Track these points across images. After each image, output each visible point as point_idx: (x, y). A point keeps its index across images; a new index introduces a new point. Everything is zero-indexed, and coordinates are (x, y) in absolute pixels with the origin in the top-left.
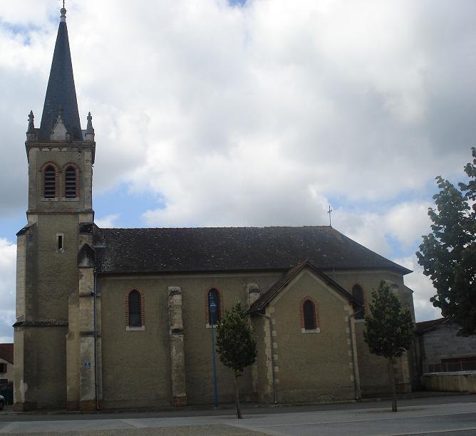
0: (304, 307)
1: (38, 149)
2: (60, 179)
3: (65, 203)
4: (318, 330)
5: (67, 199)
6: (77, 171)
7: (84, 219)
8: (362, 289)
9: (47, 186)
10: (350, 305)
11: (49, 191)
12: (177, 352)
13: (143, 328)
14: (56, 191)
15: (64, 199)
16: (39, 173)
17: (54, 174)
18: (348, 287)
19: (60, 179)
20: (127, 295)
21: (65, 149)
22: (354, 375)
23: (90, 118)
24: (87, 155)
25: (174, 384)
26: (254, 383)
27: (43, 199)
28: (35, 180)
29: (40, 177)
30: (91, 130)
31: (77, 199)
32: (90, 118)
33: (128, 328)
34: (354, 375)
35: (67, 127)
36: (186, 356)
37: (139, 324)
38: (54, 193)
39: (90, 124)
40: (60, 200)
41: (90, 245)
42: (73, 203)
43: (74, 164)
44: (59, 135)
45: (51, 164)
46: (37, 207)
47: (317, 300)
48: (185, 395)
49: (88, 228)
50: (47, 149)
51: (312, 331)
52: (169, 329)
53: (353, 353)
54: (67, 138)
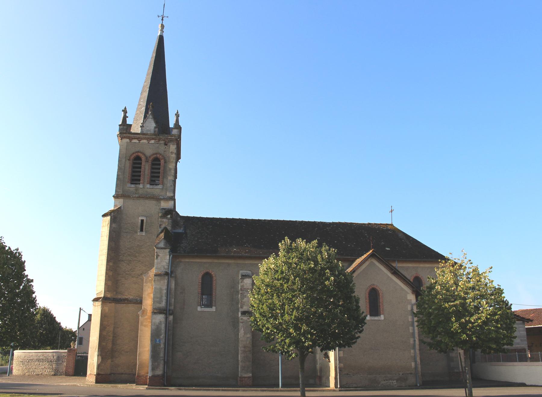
0: (369, 294)
1: (128, 140)
2: (146, 168)
3: (149, 190)
4: (382, 317)
5: (151, 187)
6: (162, 162)
7: (165, 205)
8: (421, 280)
9: (134, 174)
10: (413, 293)
11: (135, 178)
12: (245, 333)
13: (214, 309)
14: (142, 178)
15: (148, 186)
16: (128, 161)
17: (141, 164)
18: (411, 277)
19: (146, 168)
20: (200, 276)
21: (153, 141)
22: (416, 362)
23: (177, 115)
24: (173, 148)
25: (240, 364)
26: (318, 366)
27: (129, 185)
28: (123, 168)
29: (128, 164)
30: (178, 126)
31: (160, 187)
32: (177, 115)
33: (199, 309)
34: (416, 362)
35: (156, 122)
36: (253, 337)
37: (210, 305)
38: (139, 180)
39: (177, 121)
40: (145, 187)
41: (169, 228)
42: (157, 190)
43: (160, 154)
44: (148, 128)
45: (139, 154)
46: (123, 191)
47: (382, 288)
48: (251, 375)
49: (171, 212)
50: (145, 141)
51: (376, 318)
52: (239, 311)
53: (415, 341)
54: (155, 131)
